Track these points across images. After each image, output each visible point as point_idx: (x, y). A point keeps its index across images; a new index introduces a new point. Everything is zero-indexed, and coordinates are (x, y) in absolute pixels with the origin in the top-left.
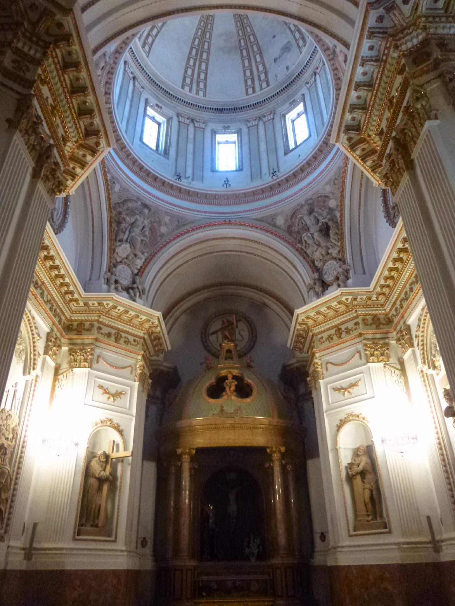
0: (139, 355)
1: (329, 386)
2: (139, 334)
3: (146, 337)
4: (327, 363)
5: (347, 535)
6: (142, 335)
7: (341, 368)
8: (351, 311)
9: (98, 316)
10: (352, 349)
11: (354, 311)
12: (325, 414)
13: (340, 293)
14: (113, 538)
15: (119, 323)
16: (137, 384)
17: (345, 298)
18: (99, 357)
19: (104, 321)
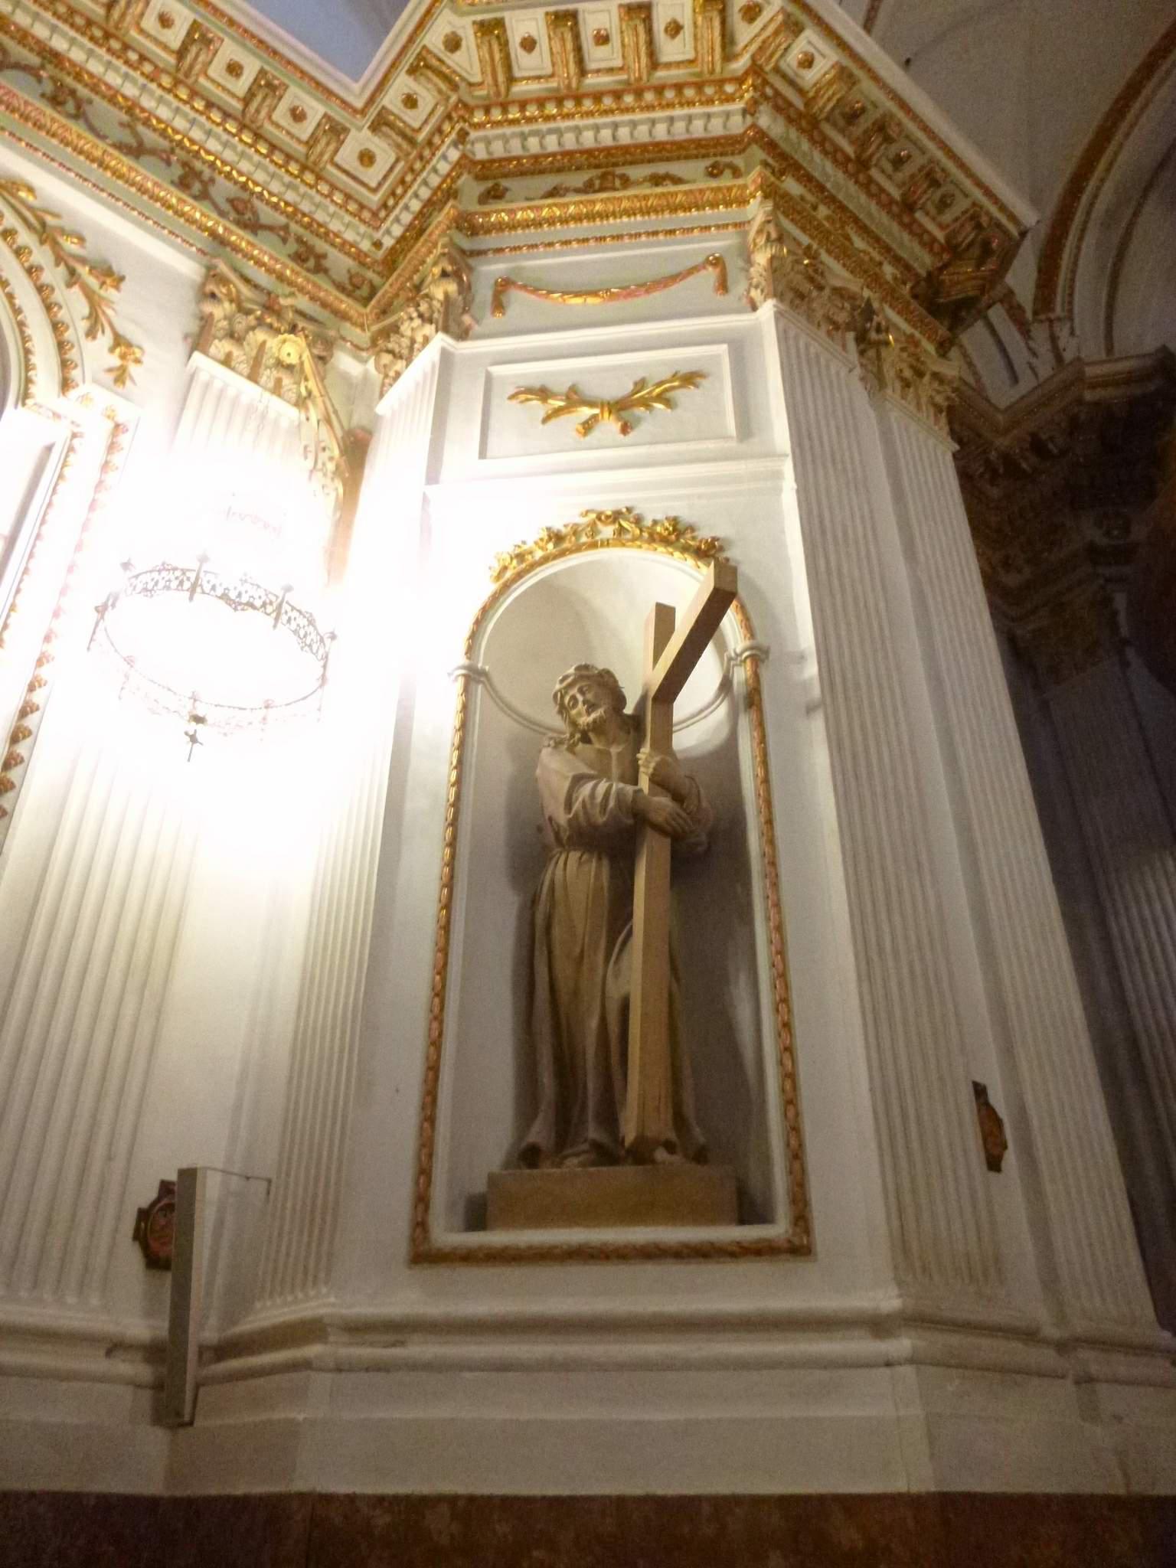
0: (743, 202)
2: (717, 128)
3: (765, 119)
6: (737, 125)
9: (455, 144)
14: (778, 1230)
15: (577, 121)
16: (768, 309)
18: (504, 286)
19: (498, 150)
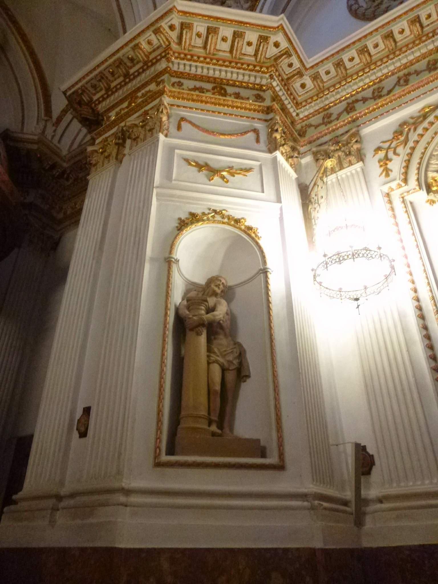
1: (177, 151)
4: (183, 119)
5: (151, 460)
7: (211, 137)
8: (263, 72)
10: (245, 123)
11: (267, 76)
12: (155, 191)
13: (276, 25)
17: (280, 38)
